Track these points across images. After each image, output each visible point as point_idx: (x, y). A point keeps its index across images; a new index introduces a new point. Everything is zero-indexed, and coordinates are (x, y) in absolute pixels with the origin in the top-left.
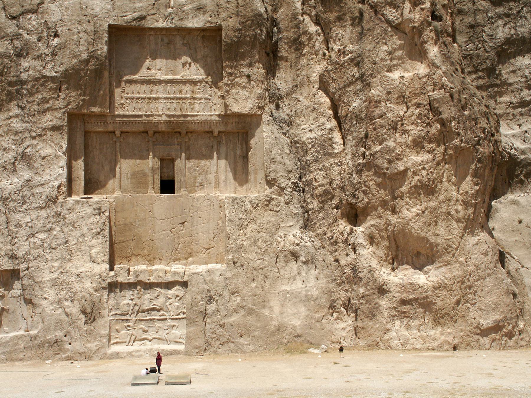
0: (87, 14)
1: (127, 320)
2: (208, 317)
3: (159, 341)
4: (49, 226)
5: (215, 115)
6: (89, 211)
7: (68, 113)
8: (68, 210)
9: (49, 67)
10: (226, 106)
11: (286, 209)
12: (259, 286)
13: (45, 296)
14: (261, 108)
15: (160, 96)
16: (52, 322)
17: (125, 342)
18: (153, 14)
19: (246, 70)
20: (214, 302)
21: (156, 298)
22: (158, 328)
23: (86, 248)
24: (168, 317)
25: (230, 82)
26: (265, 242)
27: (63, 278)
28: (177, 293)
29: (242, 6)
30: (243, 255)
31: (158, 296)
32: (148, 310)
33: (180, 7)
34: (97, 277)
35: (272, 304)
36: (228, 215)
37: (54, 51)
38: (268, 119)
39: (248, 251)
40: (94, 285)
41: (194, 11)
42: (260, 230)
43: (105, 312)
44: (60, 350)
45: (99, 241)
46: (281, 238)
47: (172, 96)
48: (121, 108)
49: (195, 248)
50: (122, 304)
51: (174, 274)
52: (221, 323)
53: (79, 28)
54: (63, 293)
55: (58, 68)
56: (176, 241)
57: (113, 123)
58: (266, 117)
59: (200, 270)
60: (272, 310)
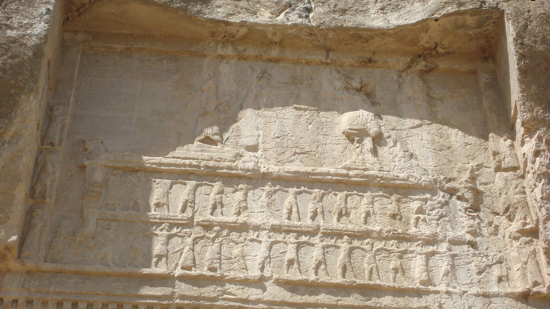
5: (507, 295)
15: (256, 219)
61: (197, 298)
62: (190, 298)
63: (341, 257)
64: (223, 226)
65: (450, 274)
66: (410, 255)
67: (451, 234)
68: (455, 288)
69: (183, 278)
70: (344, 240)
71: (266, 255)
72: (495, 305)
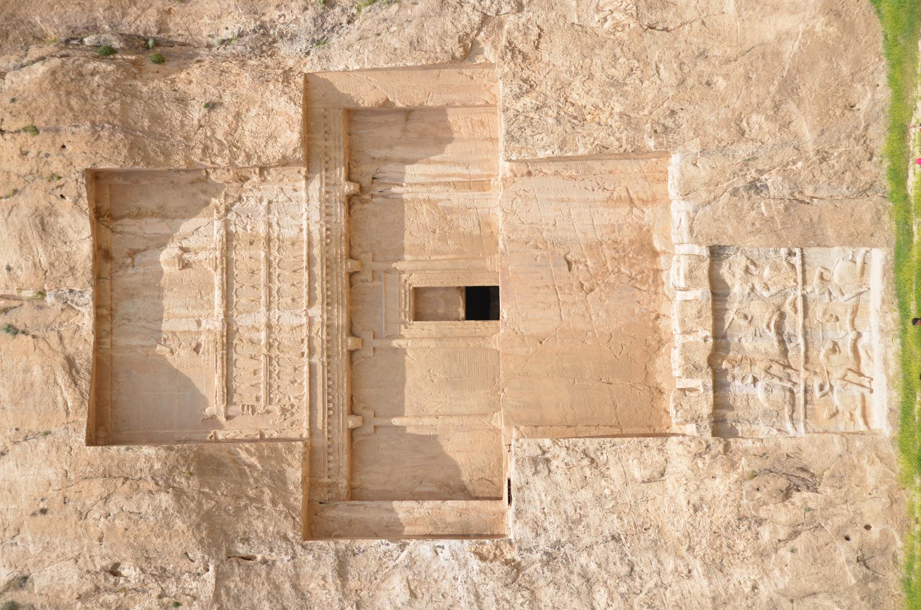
0: (60, 498)
1: (806, 391)
2: (801, 192)
3: (859, 313)
4: (577, 581)
5: (307, 188)
6: (539, 483)
7: (305, 540)
8: (537, 535)
9: (192, 585)
10: (285, 162)
11: (535, 8)
12: (724, 71)
13: (747, 590)
14: (287, 75)
15: (263, 320)
16: (813, 570)
17: (863, 396)
18: (61, 338)
19: (197, 113)
20: (763, 178)
21: (750, 321)
22: (827, 317)
23: (629, 493)
24: (799, 293)
25: (227, 152)
26: (615, 58)
27: (703, 544)
28: (739, 272)
29: (33, 118)
30: (646, 112)
31: (746, 317)
32: (782, 342)
33: (41, 273)
34: (700, 465)
35: (770, 36)
36: (549, 152)
37: (153, 575)
38: (316, 60)
39: (637, 100)
40: (718, 471)
41: (51, 240)
42: (586, 73)
43: (787, 446)
44: (883, 552)
45: (612, 460)
46: (605, 20)
47: (263, 292)
48: (292, 414)
49: (627, 235)
50: (766, 405)
51: (691, 278)
52: (815, 158)
53: (97, 516)
54: (740, 545)
55: (196, 564)
56: (612, 279)
58: (311, 66)
59: (683, 216)
60: (788, 33)
62: (322, 352)
64: (268, 337)
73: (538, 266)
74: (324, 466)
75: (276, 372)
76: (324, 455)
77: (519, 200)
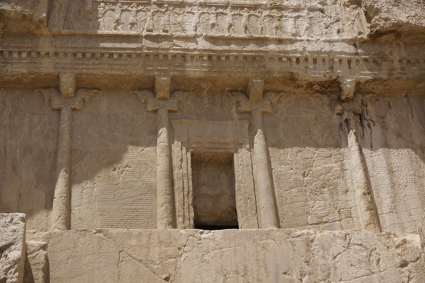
5: (343, 41)
57: (56, 54)
61: (157, 49)
63: (243, 21)
65: (309, 29)
66: (285, 18)
67: (309, 5)
68: (312, 37)
69: (147, 37)
70: (244, 11)
71: (198, 21)
72: (336, 47)
73: (277, 275)
74: (16, 47)
75: (130, 9)
76: (28, 47)
77: (364, 254)
